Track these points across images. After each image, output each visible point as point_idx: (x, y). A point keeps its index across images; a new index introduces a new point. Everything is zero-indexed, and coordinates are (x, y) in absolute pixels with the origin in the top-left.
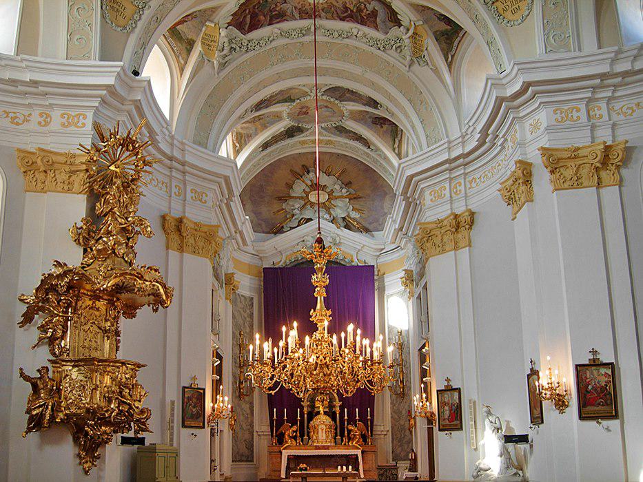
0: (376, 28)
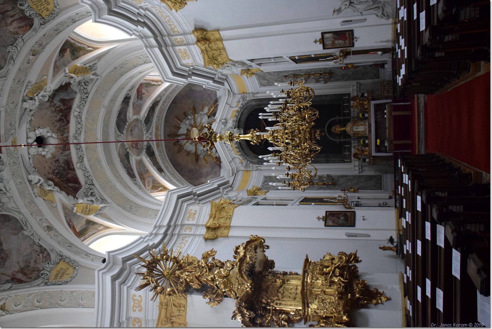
0: (73, 99)
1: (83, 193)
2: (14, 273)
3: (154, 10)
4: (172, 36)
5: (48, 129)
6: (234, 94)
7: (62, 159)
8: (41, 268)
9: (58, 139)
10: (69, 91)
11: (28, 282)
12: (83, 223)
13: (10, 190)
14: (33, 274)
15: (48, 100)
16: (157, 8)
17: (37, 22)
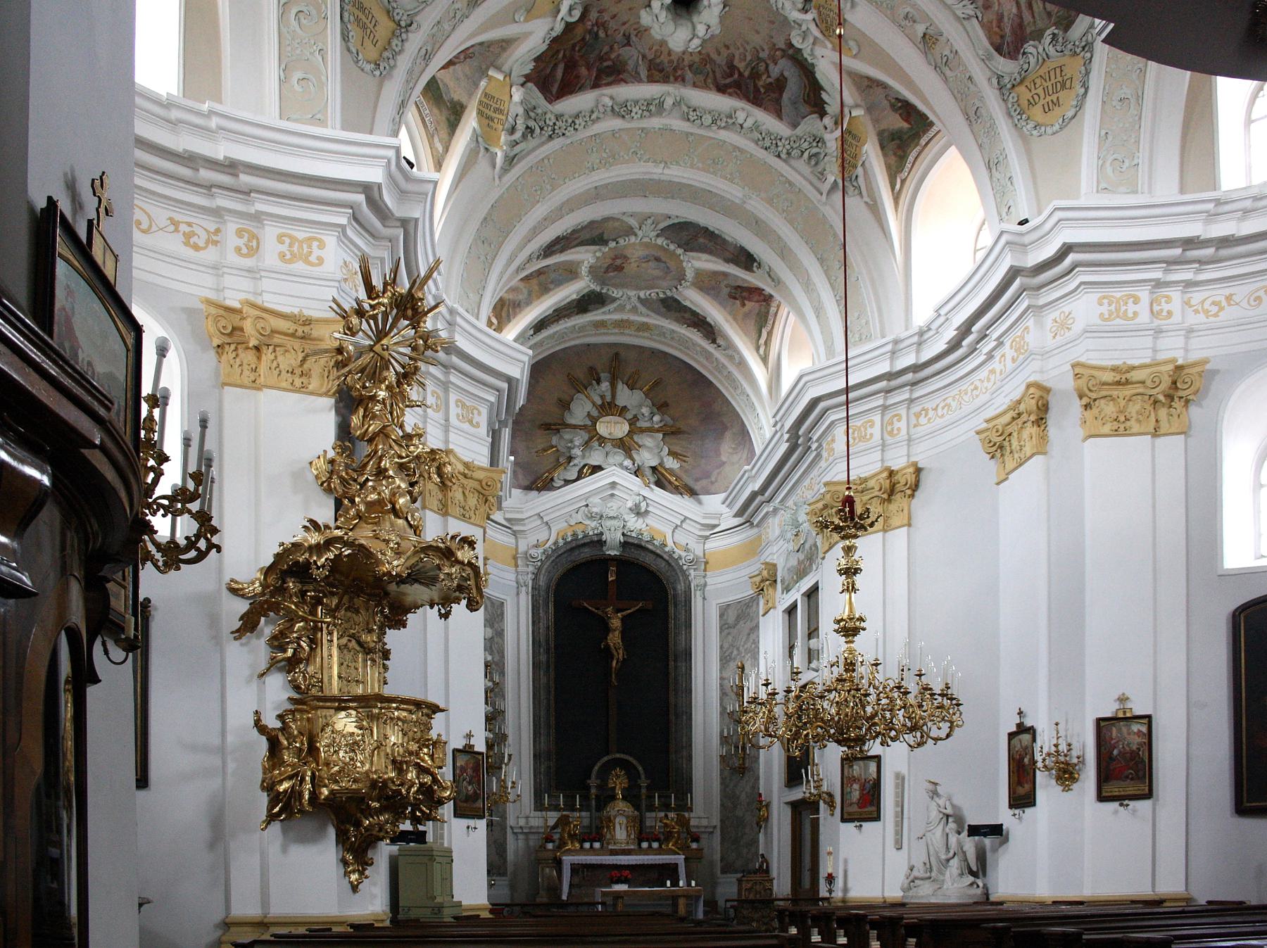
0: (779, 114)
1: (533, 103)
3: (983, 373)
4: (908, 408)
5: (716, 30)
6: (707, 538)
7: (630, 55)
9: (684, 53)
10: (804, 109)
12: (457, 94)
15: (791, 45)
16: (986, 384)
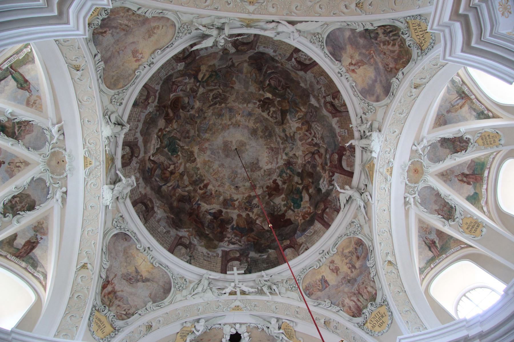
2: (113, 285)
8: (111, 309)
11: (101, 293)
13: (194, 298)
14: (107, 299)
17: (360, 320)
